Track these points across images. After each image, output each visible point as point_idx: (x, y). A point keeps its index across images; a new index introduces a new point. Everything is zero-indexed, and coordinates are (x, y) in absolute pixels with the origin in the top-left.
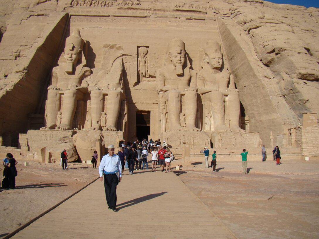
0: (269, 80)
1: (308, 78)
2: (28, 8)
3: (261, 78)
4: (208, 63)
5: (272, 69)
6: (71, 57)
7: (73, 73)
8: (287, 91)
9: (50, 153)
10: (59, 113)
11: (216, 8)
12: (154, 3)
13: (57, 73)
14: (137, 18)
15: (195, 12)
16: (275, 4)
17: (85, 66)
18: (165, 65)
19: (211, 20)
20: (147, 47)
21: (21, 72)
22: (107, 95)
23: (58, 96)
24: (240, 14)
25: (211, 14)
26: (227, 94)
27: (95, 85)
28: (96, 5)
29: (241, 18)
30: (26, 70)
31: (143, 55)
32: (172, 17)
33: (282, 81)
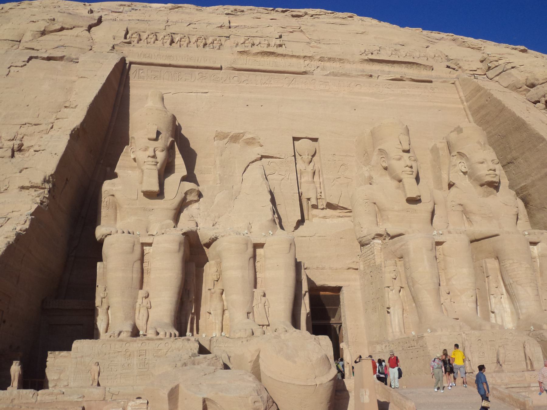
2: (20, 41)
4: (465, 173)
6: (154, 157)
7: (160, 194)
9: (204, 401)
10: (142, 293)
11: (451, 58)
13: (118, 195)
14: (286, 75)
15: (409, 65)
17: (184, 179)
18: (371, 178)
19: (445, 82)
20: (315, 140)
21: (36, 187)
22: (261, 246)
23: (138, 249)
24: (513, 68)
26: (536, 241)
27: (213, 226)
28: (185, 45)
30: (48, 182)
31: (307, 158)
32: (362, 75)
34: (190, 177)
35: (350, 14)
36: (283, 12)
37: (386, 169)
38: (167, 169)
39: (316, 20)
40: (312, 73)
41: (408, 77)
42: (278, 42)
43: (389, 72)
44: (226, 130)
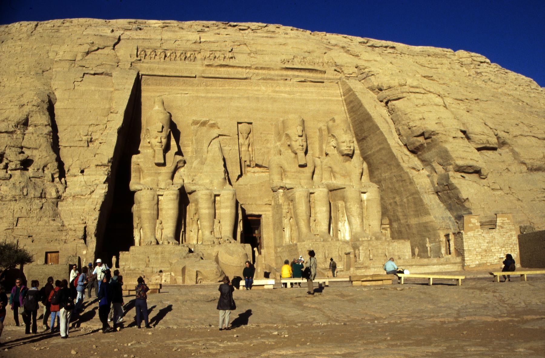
0: (417, 172)
1: (466, 171)
3: (408, 170)
5: (420, 157)
7: (164, 164)
8: (441, 186)
12: (252, 55)
16: (410, 47)
17: (177, 154)
18: (280, 151)
20: (251, 123)
22: (219, 195)
25: (330, 74)
28: (173, 59)
29: (375, 82)
33: (435, 174)
34: (179, 153)
35: (277, 25)
36: (234, 26)
37: (289, 146)
38: (167, 148)
39: (256, 34)
40: (250, 79)
41: (309, 79)
42: (230, 55)
43: (298, 76)
44: (199, 119)
